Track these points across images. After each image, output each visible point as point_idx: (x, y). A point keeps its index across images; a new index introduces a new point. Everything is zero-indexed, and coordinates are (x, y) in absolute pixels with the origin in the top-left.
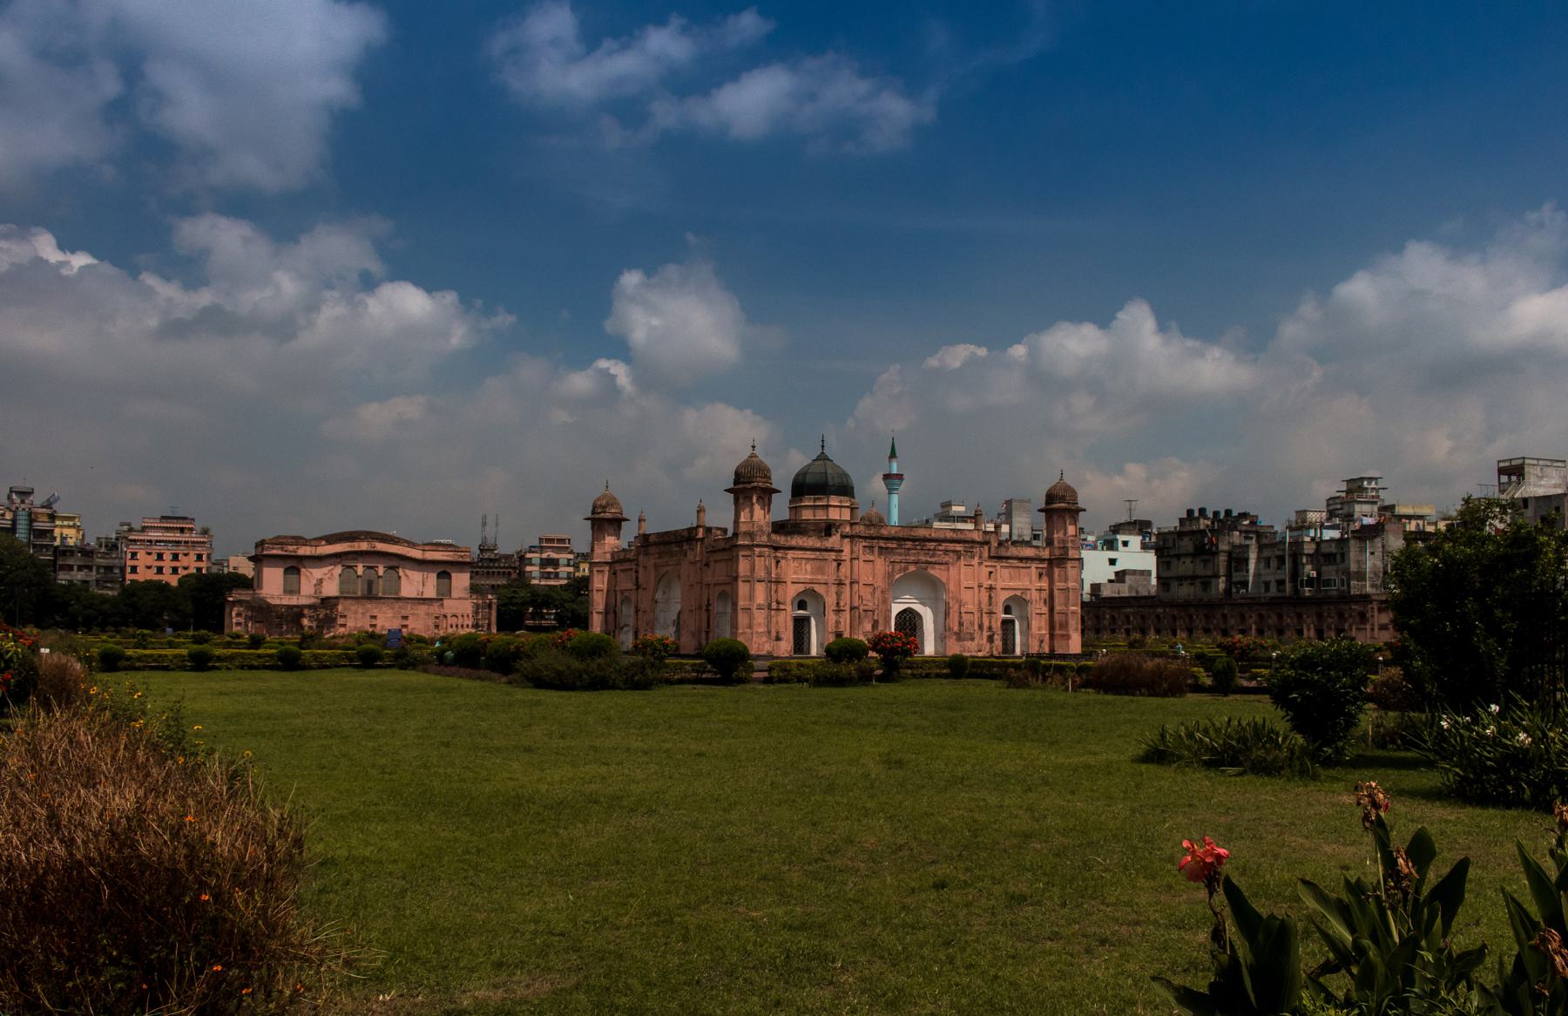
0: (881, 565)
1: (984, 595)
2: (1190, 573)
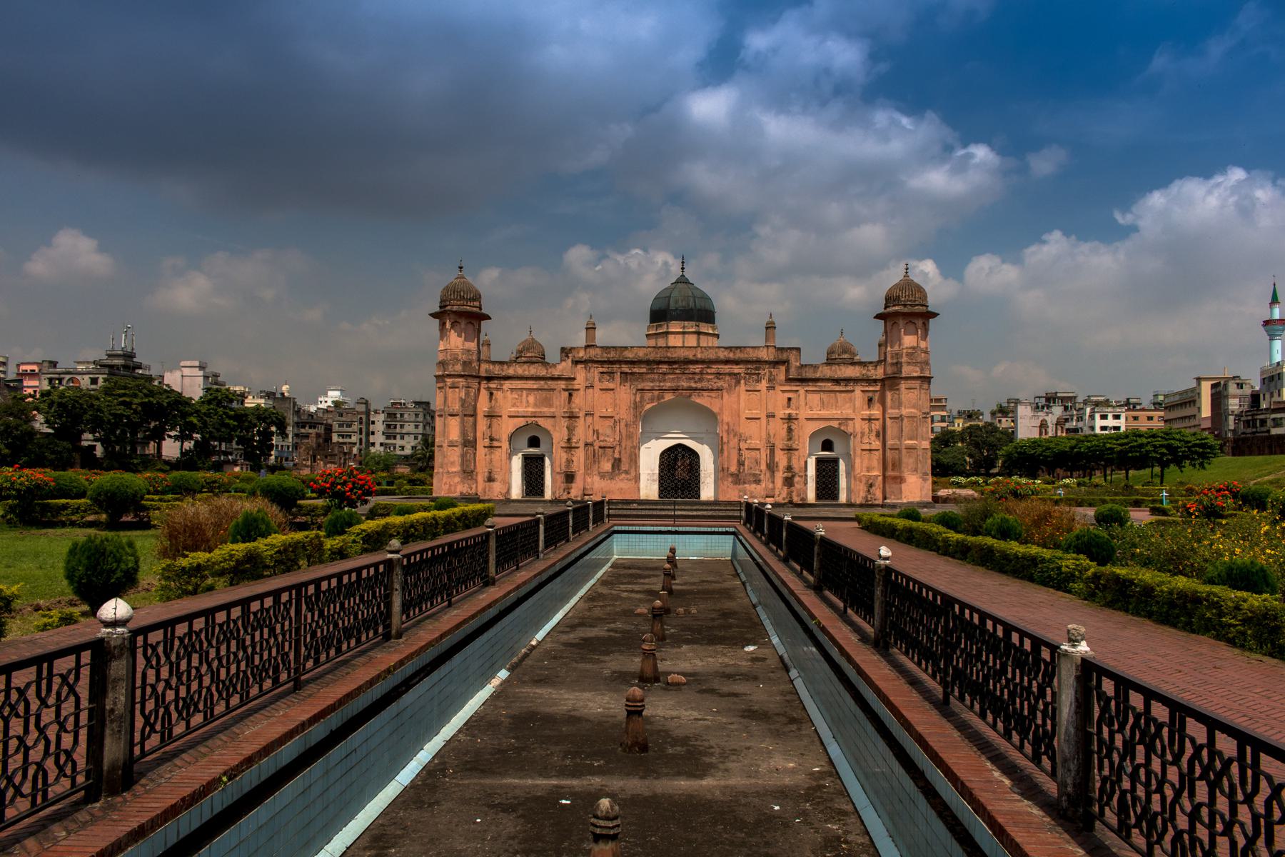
0: (625, 394)
1: (779, 429)
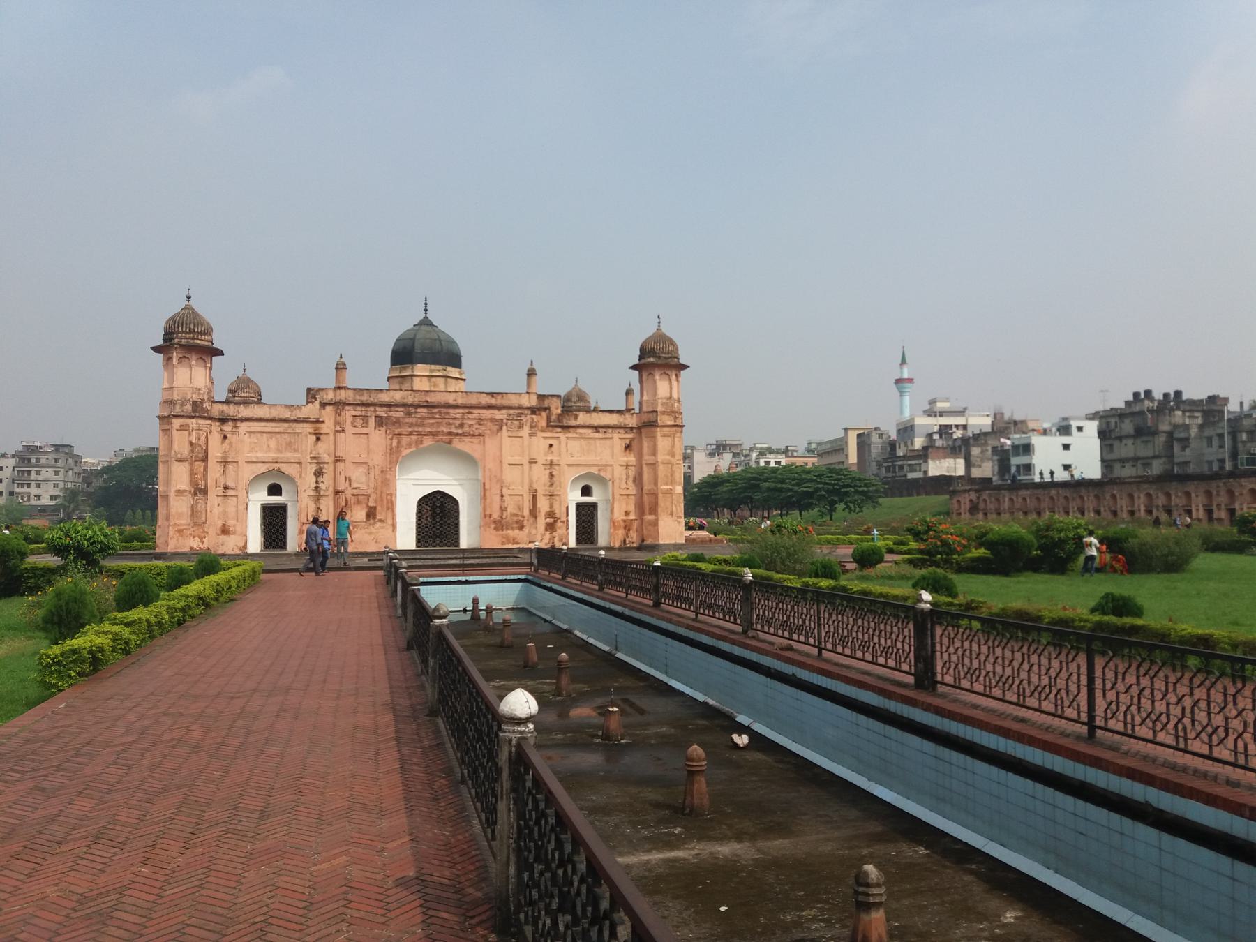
1: (540, 475)
2: (1131, 455)
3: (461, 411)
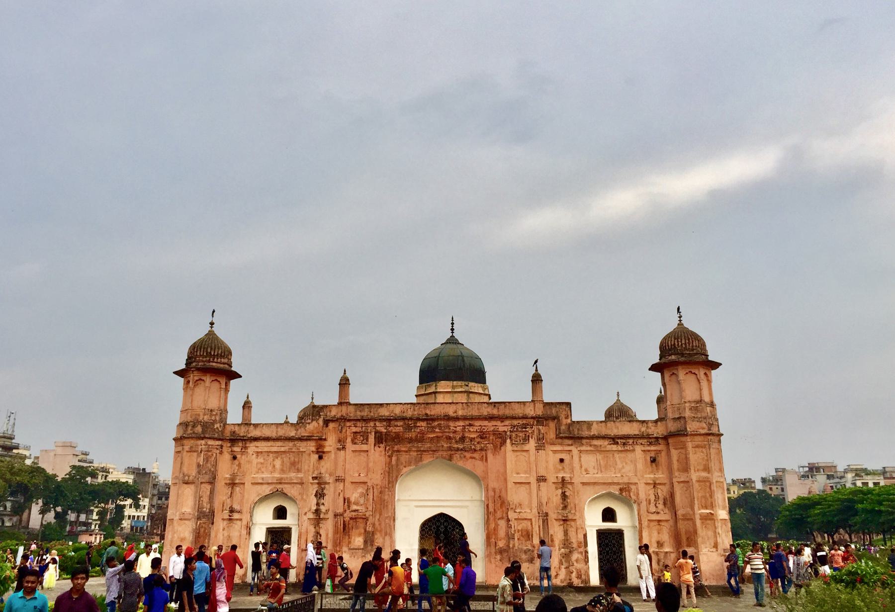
1: (551, 495)
3: (461, 423)
